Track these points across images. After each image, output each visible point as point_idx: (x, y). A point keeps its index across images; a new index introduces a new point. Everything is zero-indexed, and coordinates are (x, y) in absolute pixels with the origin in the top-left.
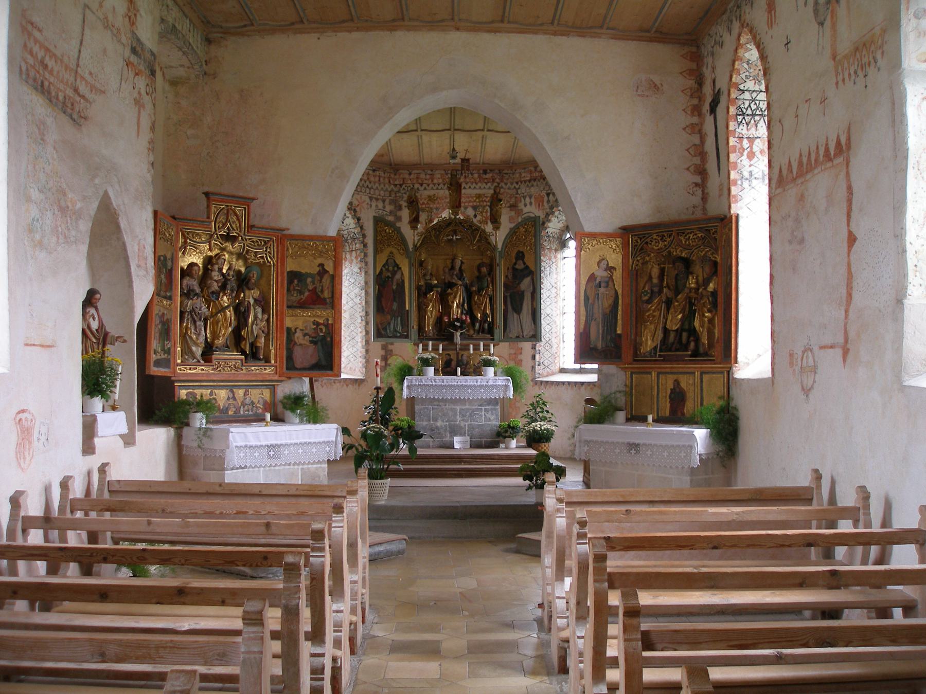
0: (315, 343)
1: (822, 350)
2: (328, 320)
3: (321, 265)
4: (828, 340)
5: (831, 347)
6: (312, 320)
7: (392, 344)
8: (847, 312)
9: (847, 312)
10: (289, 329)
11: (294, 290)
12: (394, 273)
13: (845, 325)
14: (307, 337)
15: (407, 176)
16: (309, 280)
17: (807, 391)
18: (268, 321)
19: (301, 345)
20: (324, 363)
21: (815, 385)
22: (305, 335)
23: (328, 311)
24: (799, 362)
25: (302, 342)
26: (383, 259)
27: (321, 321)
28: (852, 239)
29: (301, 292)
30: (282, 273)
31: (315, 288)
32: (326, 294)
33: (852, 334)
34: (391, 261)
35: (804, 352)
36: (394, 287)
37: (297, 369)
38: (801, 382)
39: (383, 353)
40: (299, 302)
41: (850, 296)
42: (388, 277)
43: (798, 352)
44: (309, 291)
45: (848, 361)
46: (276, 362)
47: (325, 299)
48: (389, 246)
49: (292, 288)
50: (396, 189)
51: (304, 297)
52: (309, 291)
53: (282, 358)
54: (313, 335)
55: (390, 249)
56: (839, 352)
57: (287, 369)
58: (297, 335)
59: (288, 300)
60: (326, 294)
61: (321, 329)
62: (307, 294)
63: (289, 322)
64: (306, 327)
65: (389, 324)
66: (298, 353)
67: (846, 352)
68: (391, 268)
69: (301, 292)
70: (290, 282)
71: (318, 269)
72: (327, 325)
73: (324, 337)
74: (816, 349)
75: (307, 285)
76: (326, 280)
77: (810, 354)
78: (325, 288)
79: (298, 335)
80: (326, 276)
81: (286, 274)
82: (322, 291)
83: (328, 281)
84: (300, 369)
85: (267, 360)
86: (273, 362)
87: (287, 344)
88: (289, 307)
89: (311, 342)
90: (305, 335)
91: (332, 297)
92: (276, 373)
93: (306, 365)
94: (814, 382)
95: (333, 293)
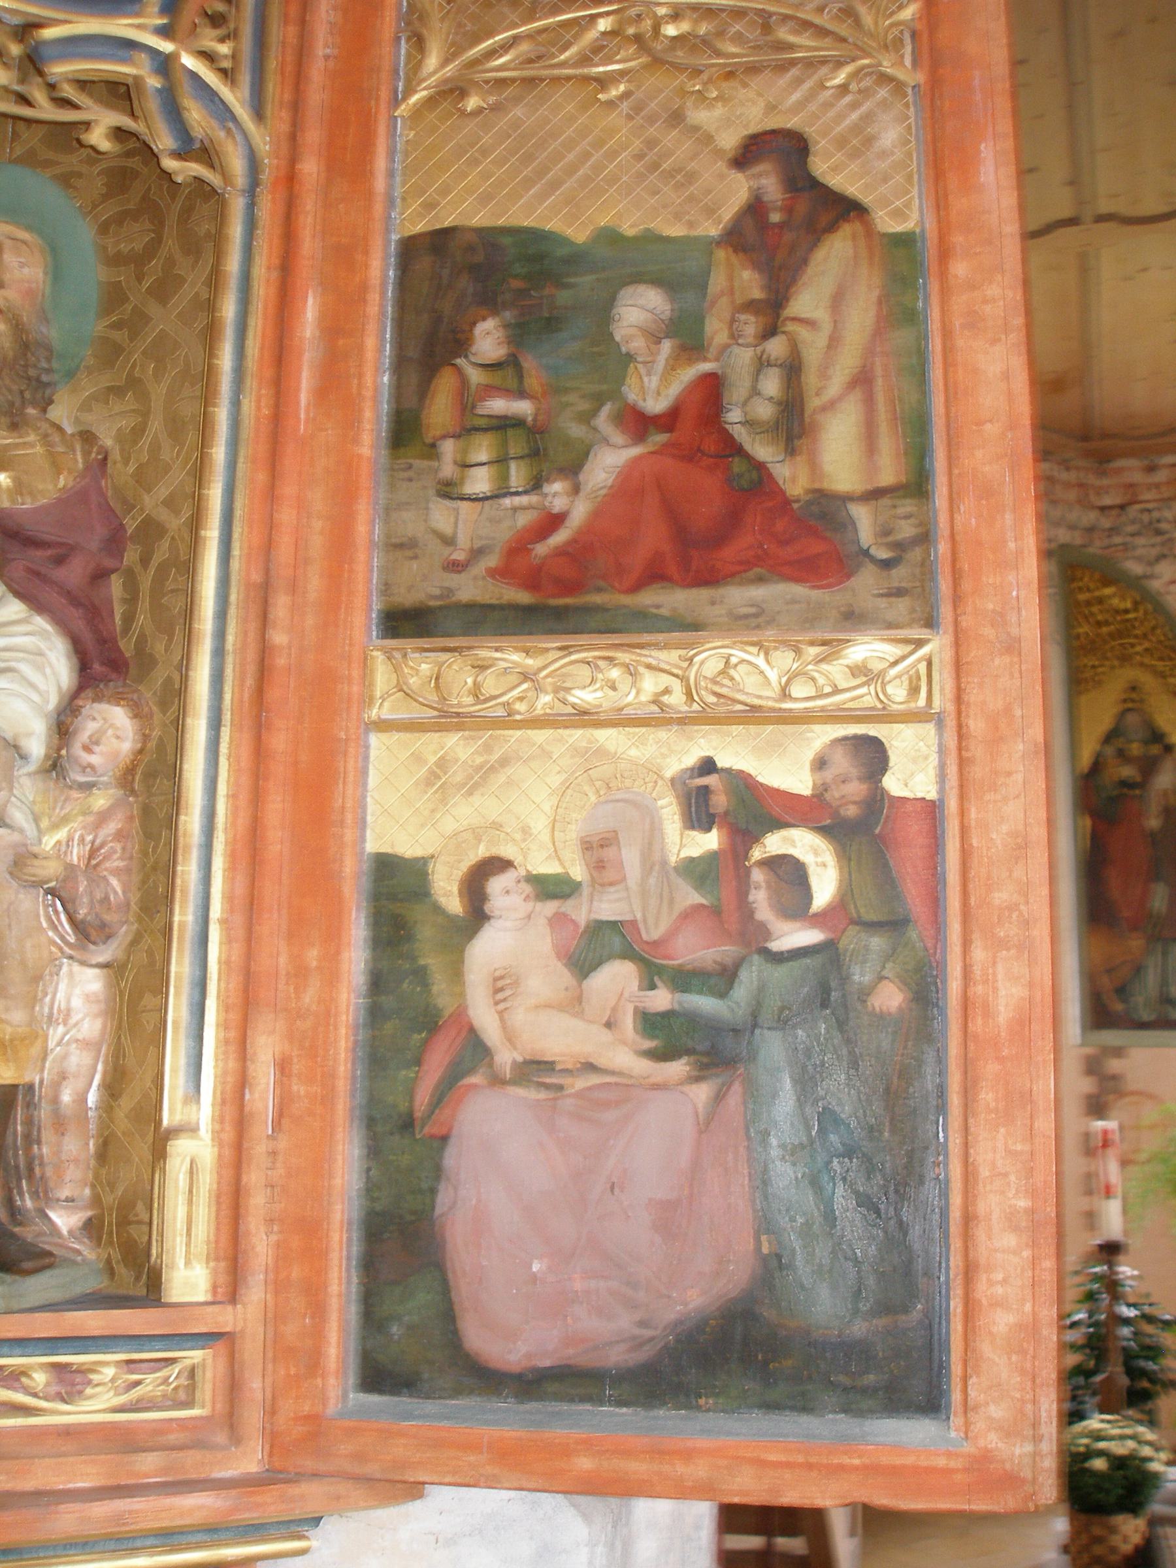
0: (696, 1043)
2: (872, 756)
3: (781, 149)
6: (683, 753)
7: (1118, 1052)
10: (396, 888)
11: (466, 431)
12: (1149, 767)
14: (617, 978)
15: (1138, 477)
16: (639, 310)
18: (153, 778)
19: (535, 1070)
20: (824, 1304)
22: (590, 948)
23: (868, 649)
25: (561, 1038)
26: (1102, 711)
27: (788, 771)
29: (542, 450)
30: (345, 254)
31: (712, 389)
32: (840, 456)
34: (1132, 719)
36: (1153, 823)
37: (487, 1379)
39: (1087, 1085)
40: (516, 564)
42: (1124, 784)
44: (638, 423)
46: (231, 1288)
47: (826, 510)
48: (1125, 659)
49: (440, 410)
50: (1106, 523)
51: (576, 503)
52: (638, 423)
53: (304, 1231)
54: (696, 949)
55: (1130, 674)
57: (378, 1376)
58: (489, 949)
59: (401, 547)
60: (840, 456)
61: (790, 874)
62: (611, 460)
63: (400, 806)
64: (599, 848)
65: (1138, 970)
66: (503, 1173)
68: (1135, 749)
69: (542, 450)
70: (429, 347)
71: (737, 191)
72: (863, 823)
73: (826, 980)
75: (611, 362)
76: (833, 294)
78: (828, 382)
79: (512, 943)
80: (836, 253)
81: (380, 270)
82: (794, 424)
83: (860, 317)
84: (533, 1384)
85: (134, 1274)
86: (189, 1278)
87: (378, 1059)
88: (405, 622)
89: (667, 1036)
90: (590, 948)
91: (917, 485)
92: (230, 1419)
93: (609, 1329)
95: (917, 432)
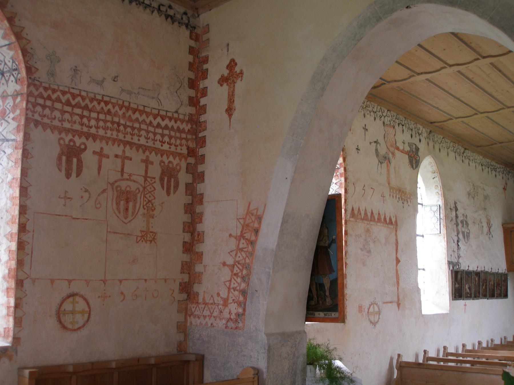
1: (385, 305)
4: (389, 299)
5: (390, 302)
8: (398, 289)
9: (398, 289)
13: (398, 294)
17: (374, 324)
21: (380, 320)
24: (366, 310)
28: (398, 261)
33: (401, 297)
35: (370, 306)
38: (369, 319)
41: (398, 283)
43: (366, 304)
45: (400, 308)
56: (395, 305)
67: (399, 305)
74: (380, 304)
77: (375, 306)
94: (379, 318)
